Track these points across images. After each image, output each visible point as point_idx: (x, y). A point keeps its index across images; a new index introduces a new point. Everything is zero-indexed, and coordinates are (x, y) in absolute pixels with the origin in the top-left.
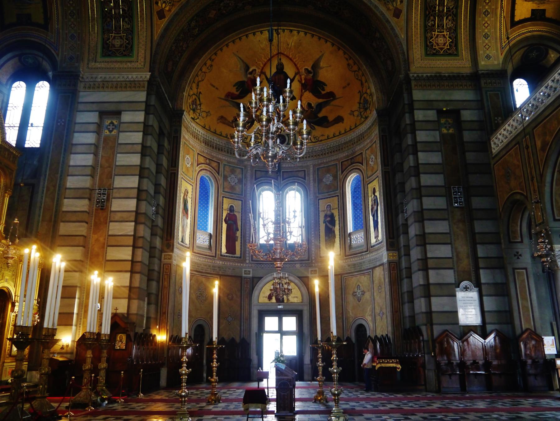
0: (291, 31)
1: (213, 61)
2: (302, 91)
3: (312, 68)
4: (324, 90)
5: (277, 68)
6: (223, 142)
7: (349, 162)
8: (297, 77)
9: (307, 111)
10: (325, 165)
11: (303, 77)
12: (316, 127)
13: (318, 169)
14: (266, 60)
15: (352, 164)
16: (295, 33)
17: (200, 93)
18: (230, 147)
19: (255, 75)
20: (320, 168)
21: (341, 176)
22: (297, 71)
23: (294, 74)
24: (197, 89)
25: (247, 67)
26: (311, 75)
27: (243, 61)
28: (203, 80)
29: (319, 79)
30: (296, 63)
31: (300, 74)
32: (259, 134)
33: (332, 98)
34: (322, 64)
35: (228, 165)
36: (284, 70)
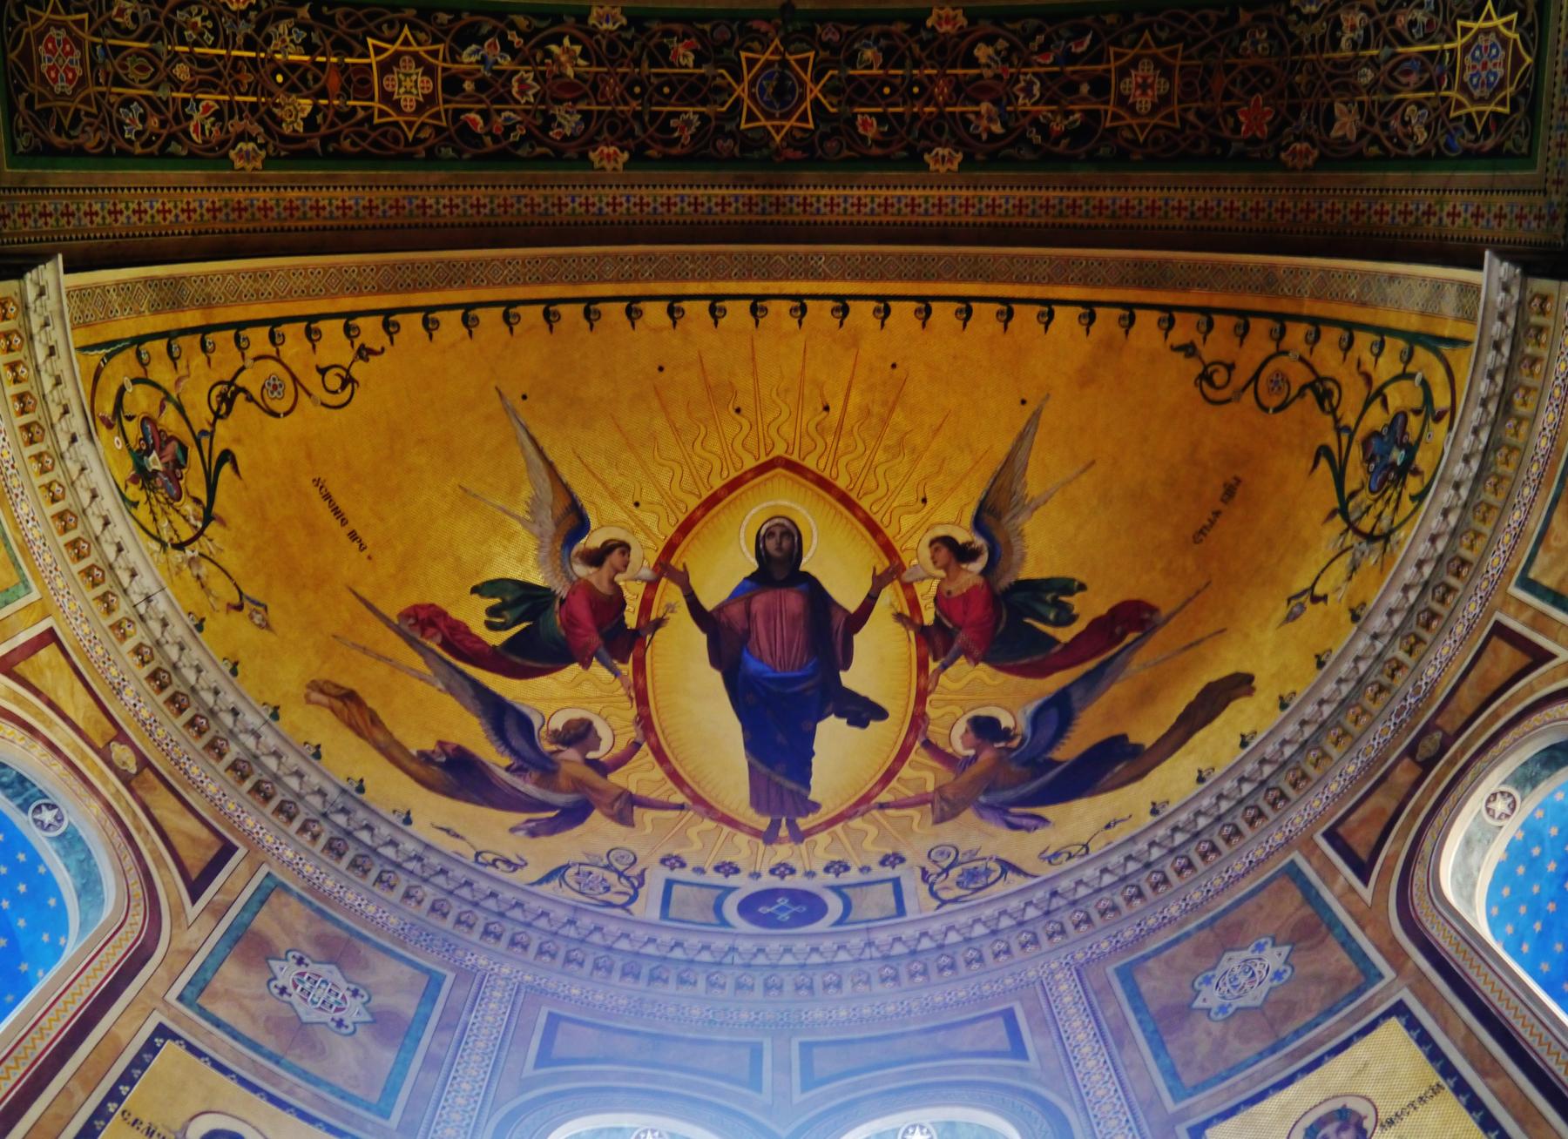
0: (842, 305)
1: (364, 353)
2: (922, 666)
3: (978, 524)
4: (1067, 618)
5: (758, 557)
8: (890, 597)
9: (970, 761)
11: (926, 591)
12: (1047, 811)
16: (862, 312)
17: (227, 456)
19: (620, 579)
22: (883, 564)
23: (866, 586)
24: (217, 415)
26: (977, 566)
27: (551, 467)
28: (276, 415)
29: (1029, 571)
31: (906, 577)
33: (1130, 638)
34: (1033, 485)
35: (301, 899)
36: (805, 566)
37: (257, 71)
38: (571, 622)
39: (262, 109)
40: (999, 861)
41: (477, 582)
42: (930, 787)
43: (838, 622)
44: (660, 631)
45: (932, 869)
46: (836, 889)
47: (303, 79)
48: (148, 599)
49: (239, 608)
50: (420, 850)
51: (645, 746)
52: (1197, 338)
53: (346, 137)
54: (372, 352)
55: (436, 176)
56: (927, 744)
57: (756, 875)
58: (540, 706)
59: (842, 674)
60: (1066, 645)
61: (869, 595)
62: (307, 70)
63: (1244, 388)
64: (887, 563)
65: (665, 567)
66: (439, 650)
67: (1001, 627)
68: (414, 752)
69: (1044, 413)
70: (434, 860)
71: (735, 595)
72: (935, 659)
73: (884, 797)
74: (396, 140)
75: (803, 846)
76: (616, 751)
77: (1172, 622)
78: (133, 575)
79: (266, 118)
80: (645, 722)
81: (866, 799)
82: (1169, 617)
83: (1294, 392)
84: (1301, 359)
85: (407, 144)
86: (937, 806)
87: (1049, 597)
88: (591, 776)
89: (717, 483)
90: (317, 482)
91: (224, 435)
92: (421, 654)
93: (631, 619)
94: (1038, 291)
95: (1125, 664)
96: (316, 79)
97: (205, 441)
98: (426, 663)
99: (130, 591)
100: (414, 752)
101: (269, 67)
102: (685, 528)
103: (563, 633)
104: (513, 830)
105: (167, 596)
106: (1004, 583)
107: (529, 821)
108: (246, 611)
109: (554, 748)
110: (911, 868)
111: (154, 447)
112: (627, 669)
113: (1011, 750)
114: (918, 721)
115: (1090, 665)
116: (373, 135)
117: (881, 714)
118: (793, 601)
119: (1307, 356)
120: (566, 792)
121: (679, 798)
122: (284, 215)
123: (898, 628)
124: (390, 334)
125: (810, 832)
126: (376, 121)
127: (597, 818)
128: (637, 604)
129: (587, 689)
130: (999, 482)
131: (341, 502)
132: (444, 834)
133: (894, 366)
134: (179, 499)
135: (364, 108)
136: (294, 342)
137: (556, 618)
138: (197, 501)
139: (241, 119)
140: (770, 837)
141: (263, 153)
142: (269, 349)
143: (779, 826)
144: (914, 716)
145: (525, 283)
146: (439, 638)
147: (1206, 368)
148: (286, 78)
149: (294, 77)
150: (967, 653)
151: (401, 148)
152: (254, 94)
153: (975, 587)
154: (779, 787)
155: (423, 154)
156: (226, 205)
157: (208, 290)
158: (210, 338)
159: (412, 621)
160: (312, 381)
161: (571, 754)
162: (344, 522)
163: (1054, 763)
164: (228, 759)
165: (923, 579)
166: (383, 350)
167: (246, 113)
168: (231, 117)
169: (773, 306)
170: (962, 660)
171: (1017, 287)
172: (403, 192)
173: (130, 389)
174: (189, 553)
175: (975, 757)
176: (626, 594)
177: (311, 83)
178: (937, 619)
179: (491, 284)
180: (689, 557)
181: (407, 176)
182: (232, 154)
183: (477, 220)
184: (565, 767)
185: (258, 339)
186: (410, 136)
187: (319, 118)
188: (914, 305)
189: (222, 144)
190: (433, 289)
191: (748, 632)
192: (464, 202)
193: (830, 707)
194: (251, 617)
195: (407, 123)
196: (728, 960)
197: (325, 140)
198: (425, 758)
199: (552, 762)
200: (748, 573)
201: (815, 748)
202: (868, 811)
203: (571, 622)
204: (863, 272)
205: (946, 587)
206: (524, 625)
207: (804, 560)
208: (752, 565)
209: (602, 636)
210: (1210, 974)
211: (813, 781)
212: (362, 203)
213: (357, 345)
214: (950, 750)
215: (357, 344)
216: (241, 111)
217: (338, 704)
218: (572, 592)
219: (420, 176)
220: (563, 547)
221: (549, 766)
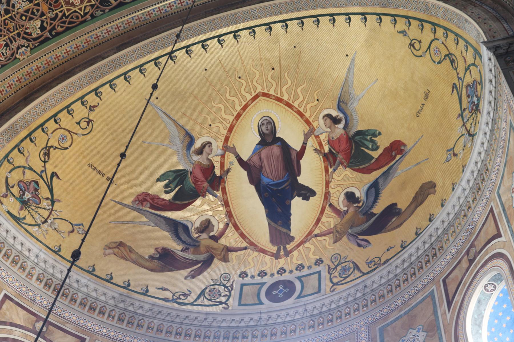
0: (269, 26)
1: (92, 108)
2: (327, 171)
5: (260, 134)
6: (110, 294)
7: (465, 264)
8: (312, 143)
10: (400, 311)
11: (323, 137)
13: (382, 331)
14: (231, 118)
15: (471, 262)
16: (278, 28)
17: (54, 174)
18: (131, 308)
19: (210, 157)
20: (388, 325)
21: (448, 316)
22: (307, 129)
23: (302, 139)
24: (45, 162)
25: (191, 141)
26: (341, 125)
27: (174, 121)
28: (67, 148)
29: (361, 127)
30: (301, 110)
31: (316, 133)
32: (224, 286)
33: (398, 157)
37: (14, 20)
38: (196, 180)
39: (22, 33)
40: (354, 263)
41: (158, 177)
42: (332, 226)
43: (294, 156)
44: (229, 174)
45: (332, 266)
46: (299, 278)
47: (33, 13)
48: (37, 256)
49: (73, 231)
50: (150, 306)
51: (230, 224)
52: (406, 28)
53: (58, 26)
54: (95, 107)
55: (98, 23)
56: (331, 205)
57: (272, 275)
58: (190, 219)
59: (298, 177)
60: (377, 159)
61: (304, 143)
62: (33, 9)
63: (426, 52)
64: (308, 128)
65: (226, 148)
66: (149, 210)
67: (353, 151)
68: (147, 257)
69: (355, 61)
70: (156, 309)
71: (254, 152)
72: (331, 168)
73: (317, 232)
74: (77, 18)
75: (289, 258)
76: (220, 230)
77: (412, 151)
78: (29, 250)
79: (25, 35)
80: (229, 214)
81: (310, 233)
82: (411, 149)
83: (443, 57)
84: (443, 43)
85: (82, 17)
86: (335, 234)
87: (369, 138)
88: (212, 243)
89: (239, 108)
90: (90, 165)
91: (50, 169)
92: (143, 214)
93: (218, 172)
94: (343, 10)
95: (396, 170)
96: (38, 11)
97: (44, 175)
98: (146, 217)
99: (30, 257)
100: (147, 257)
101: (18, 16)
102: (231, 129)
103: (194, 186)
104: (186, 278)
105: (44, 252)
106: (352, 133)
107: (191, 271)
108: (76, 231)
109: (197, 235)
110: (325, 266)
111: (25, 190)
112: (219, 193)
113: (359, 207)
114: (327, 195)
115: (385, 169)
116: (68, 20)
117: (313, 193)
118: (276, 150)
119: (445, 42)
120: (205, 253)
121: (245, 244)
122: (46, 66)
123: (316, 155)
124: (99, 97)
125: (291, 251)
126: (67, 14)
127: (216, 262)
128: (219, 165)
129: (207, 206)
130: (344, 90)
131: (100, 168)
132: (161, 290)
133: (295, 47)
134: (40, 203)
135: (61, 12)
136: (64, 118)
137: (190, 180)
138: (47, 199)
139: (16, 41)
140: (276, 256)
141: (29, 49)
142: (57, 126)
143: (280, 250)
144: (325, 193)
145: (144, 56)
146: (149, 205)
147: (411, 41)
148: (26, 16)
149: (29, 15)
150: (342, 163)
151: (81, 19)
152: (17, 29)
153: (342, 134)
154: (279, 231)
155: (90, 18)
156: (23, 75)
157: (26, 120)
158: (32, 137)
159: (137, 202)
160: (76, 129)
161: (204, 236)
162: (103, 175)
163: (373, 215)
164: (78, 301)
165: (322, 133)
166: (98, 103)
167: (17, 38)
168: (11, 43)
169: (242, 33)
170: (340, 167)
171: (334, 9)
172: (88, 35)
173: (9, 176)
174: (49, 221)
175: (347, 211)
176: (214, 162)
177: (36, 13)
178: (330, 150)
179: (131, 61)
180: (234, 141)
181: (86, 28)
182: (18, 56)
183: (120, 33)
184: (203, 243)
185: (51, 125)
186: (82, 14)
187: (45, 24)
188: (296, 21)
189: (12, 55)
190: (110, 73)
191: (261, 167)
192: (112, 28)
193: (295, 193)
194: (78, 232)
195: (79, 9)
196: (259, 323)
197: (50, 32)
198: (152, 258)
199: (198, 242)
200: (257, 142)
201: (292, 212)
202: (311, 239)
203: (196, 180)
204: (273, 12)
205: (331, 136)
206: (179, 187)
207: (277, 132)
208: (258, 139)
209: (208, 183)
210: (404, 338)
211: (292, 227)
212: (73, 47)
213: (88, 108)
214: (338, 208)
215: (88, 106)
216: (14, 39)
217: (116, 250)
218: (194, 168)
219: (92, 26)
220: (186, 151)
221: (197, 244)
